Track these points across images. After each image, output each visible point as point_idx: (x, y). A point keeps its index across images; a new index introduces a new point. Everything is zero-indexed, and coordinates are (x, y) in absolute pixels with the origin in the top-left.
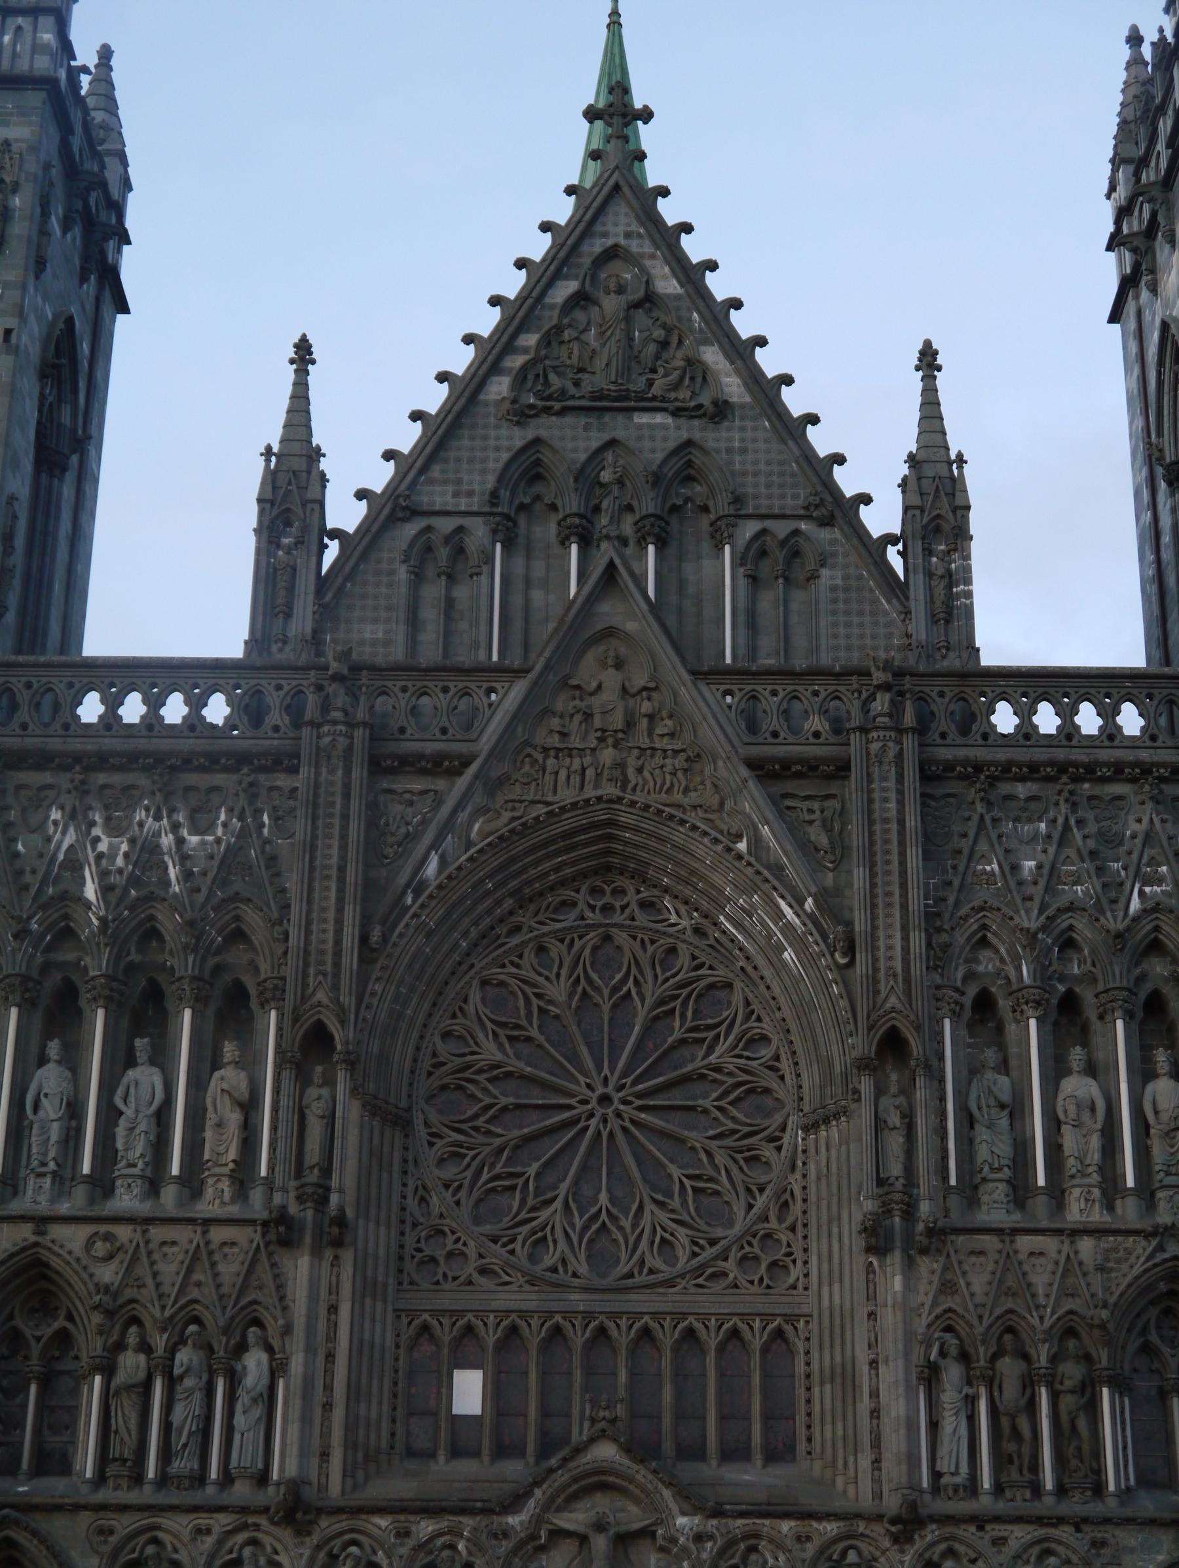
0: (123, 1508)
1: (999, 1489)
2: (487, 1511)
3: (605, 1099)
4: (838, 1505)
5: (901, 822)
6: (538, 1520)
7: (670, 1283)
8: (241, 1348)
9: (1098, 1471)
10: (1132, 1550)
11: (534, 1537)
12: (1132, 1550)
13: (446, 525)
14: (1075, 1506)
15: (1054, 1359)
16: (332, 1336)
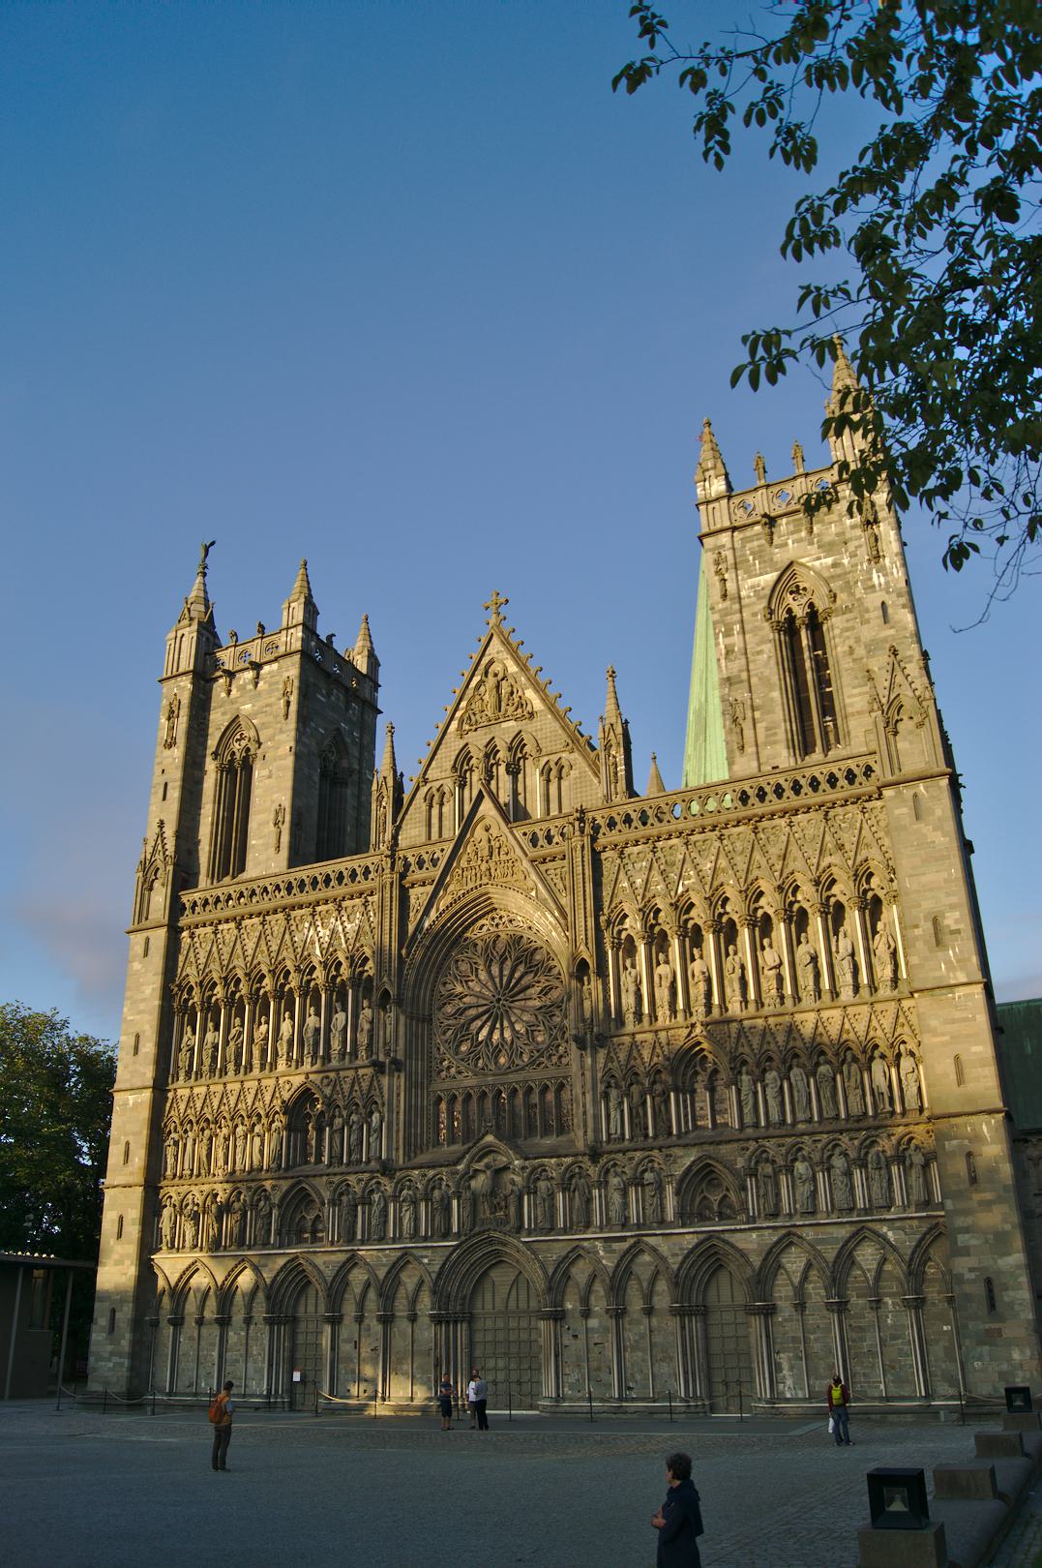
0: (335, 1174)
1: (631, 1139)
2: (447, 1166)
3: (499, 1000)
4: (572, 1150)
5: (584, 874)
6: (468, 1166)
7: (523, 1069)
8: (372, 1113)
9: (670, 1127)
10: (681, 1157)
11: (466, 1174)
12: (681, 1157)
13: (437, 784)
14: (661, 1141)
15: (654, 1083)
16: (398, 1106)
